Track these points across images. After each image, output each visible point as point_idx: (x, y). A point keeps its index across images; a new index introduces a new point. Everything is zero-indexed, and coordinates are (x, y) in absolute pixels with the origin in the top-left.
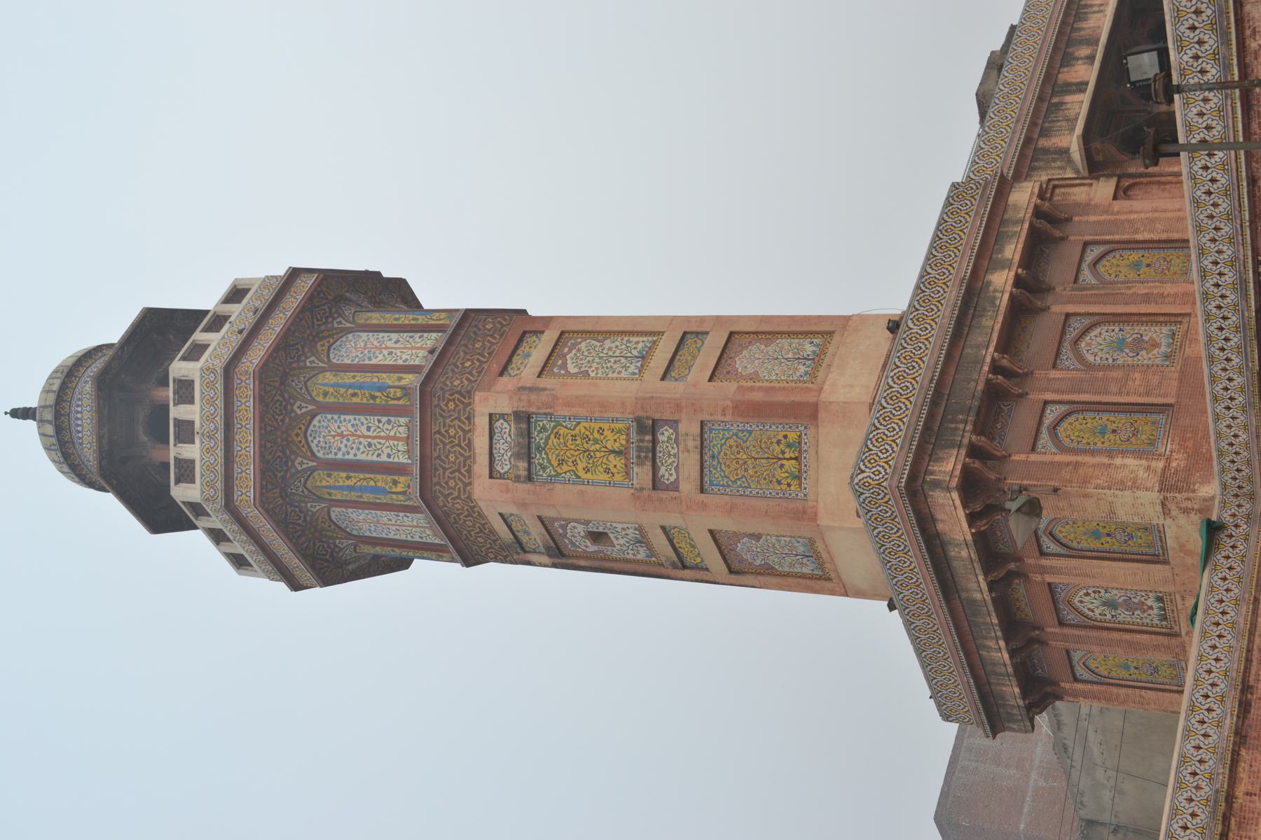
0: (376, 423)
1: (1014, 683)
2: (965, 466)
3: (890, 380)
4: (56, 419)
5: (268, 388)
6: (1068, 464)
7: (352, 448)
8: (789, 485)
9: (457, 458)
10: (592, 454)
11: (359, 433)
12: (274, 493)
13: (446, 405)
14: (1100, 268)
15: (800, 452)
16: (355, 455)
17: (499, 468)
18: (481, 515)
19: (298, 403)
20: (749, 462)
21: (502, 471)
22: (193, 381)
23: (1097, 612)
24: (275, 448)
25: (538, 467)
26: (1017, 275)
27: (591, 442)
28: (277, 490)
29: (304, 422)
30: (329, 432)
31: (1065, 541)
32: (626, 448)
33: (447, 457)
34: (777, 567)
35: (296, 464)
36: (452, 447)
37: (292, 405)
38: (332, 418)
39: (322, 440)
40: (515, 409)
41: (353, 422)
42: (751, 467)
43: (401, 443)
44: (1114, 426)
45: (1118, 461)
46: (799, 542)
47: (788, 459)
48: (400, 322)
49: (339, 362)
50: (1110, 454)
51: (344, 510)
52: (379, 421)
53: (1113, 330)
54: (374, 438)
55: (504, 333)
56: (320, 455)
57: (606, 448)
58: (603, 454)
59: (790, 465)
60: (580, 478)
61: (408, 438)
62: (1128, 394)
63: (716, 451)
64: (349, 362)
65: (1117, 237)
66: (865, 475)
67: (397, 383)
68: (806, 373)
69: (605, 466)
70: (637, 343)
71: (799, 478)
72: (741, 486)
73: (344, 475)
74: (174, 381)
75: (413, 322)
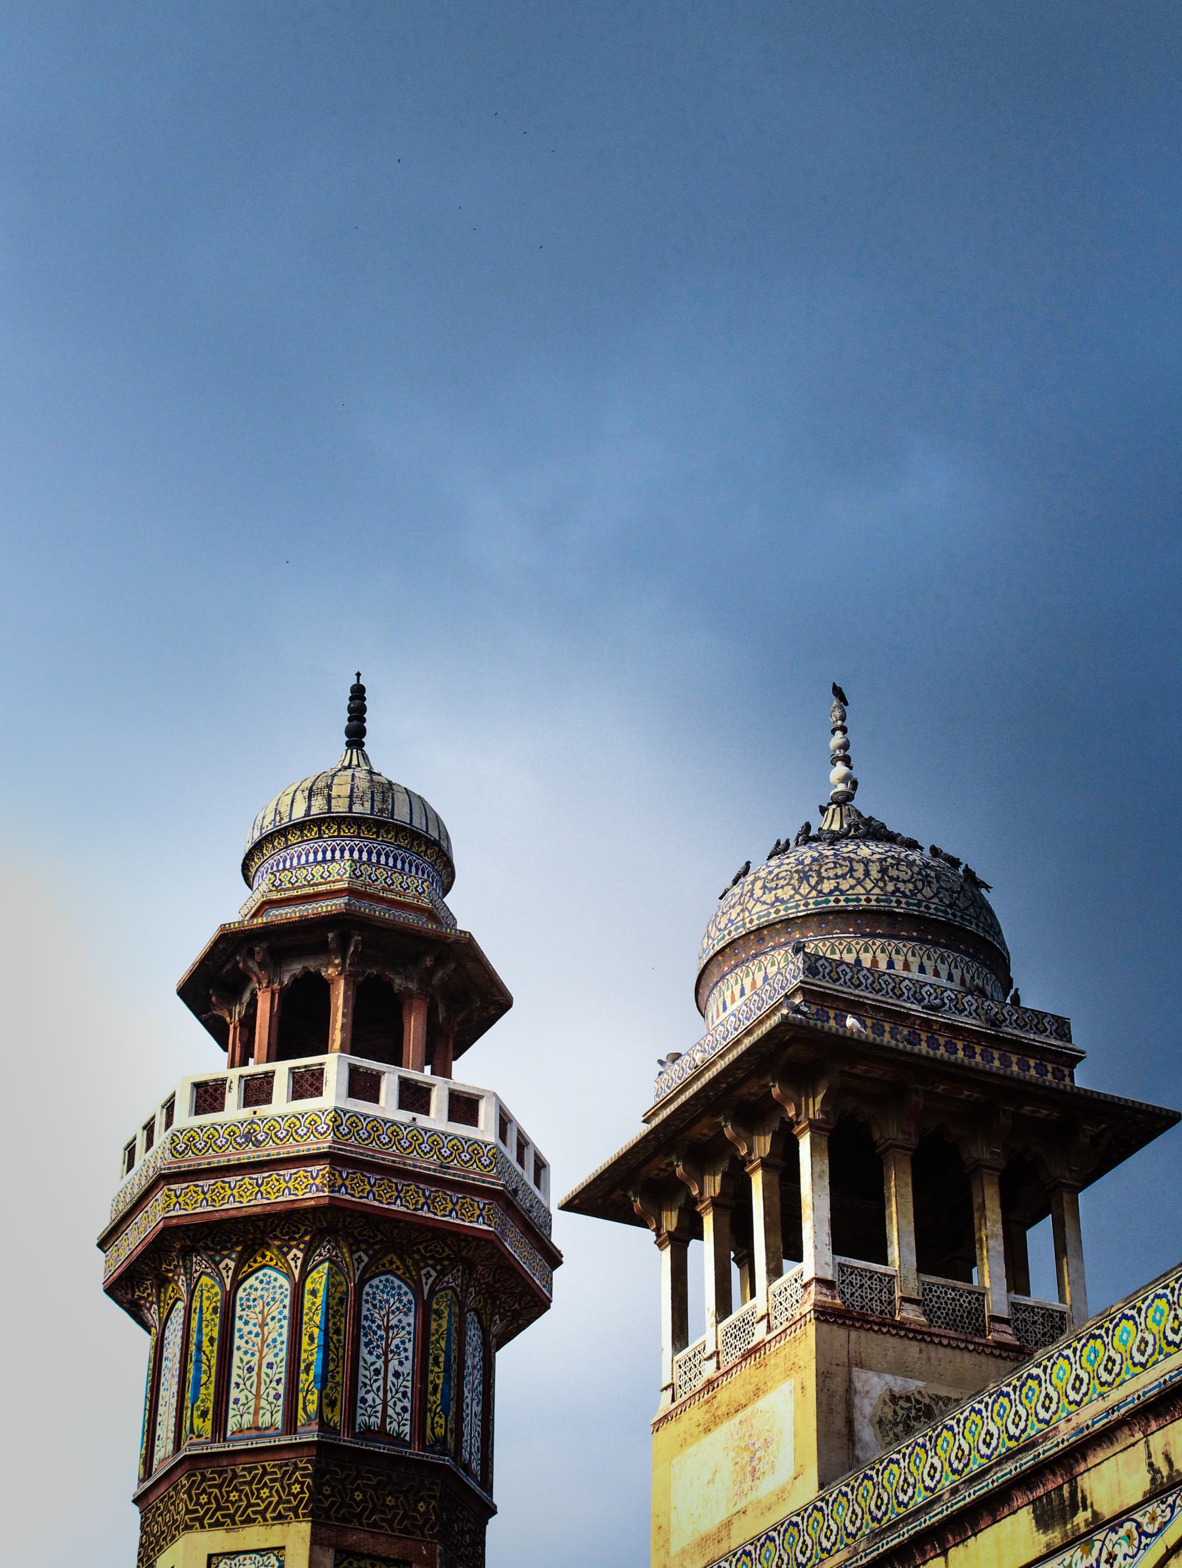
0: (277, 1377)
7: (247, 1342)
9: (233, 1503)
11: (266, 1350)
13: (297, 1481)
19: (300, 1255)
22: (321, 1094)
29: (280, 1264)
30: (268, 1304)
33: (235, 1489)
37: (297, 1247)
38: (285, 1307)
39: (259, 1293)
41: (279, 1339)
43: (251, 1417)
48: (431, 1368)
49: (364, 1297)
52: (278, 1381)
55: (409, 1533)
56: (241, 1293)
61: (258, 1428)
64: (364, 1312)
67: (325, 1401)
73: (216, 1335)
74: (321, 1064)
75: (430, 1387)
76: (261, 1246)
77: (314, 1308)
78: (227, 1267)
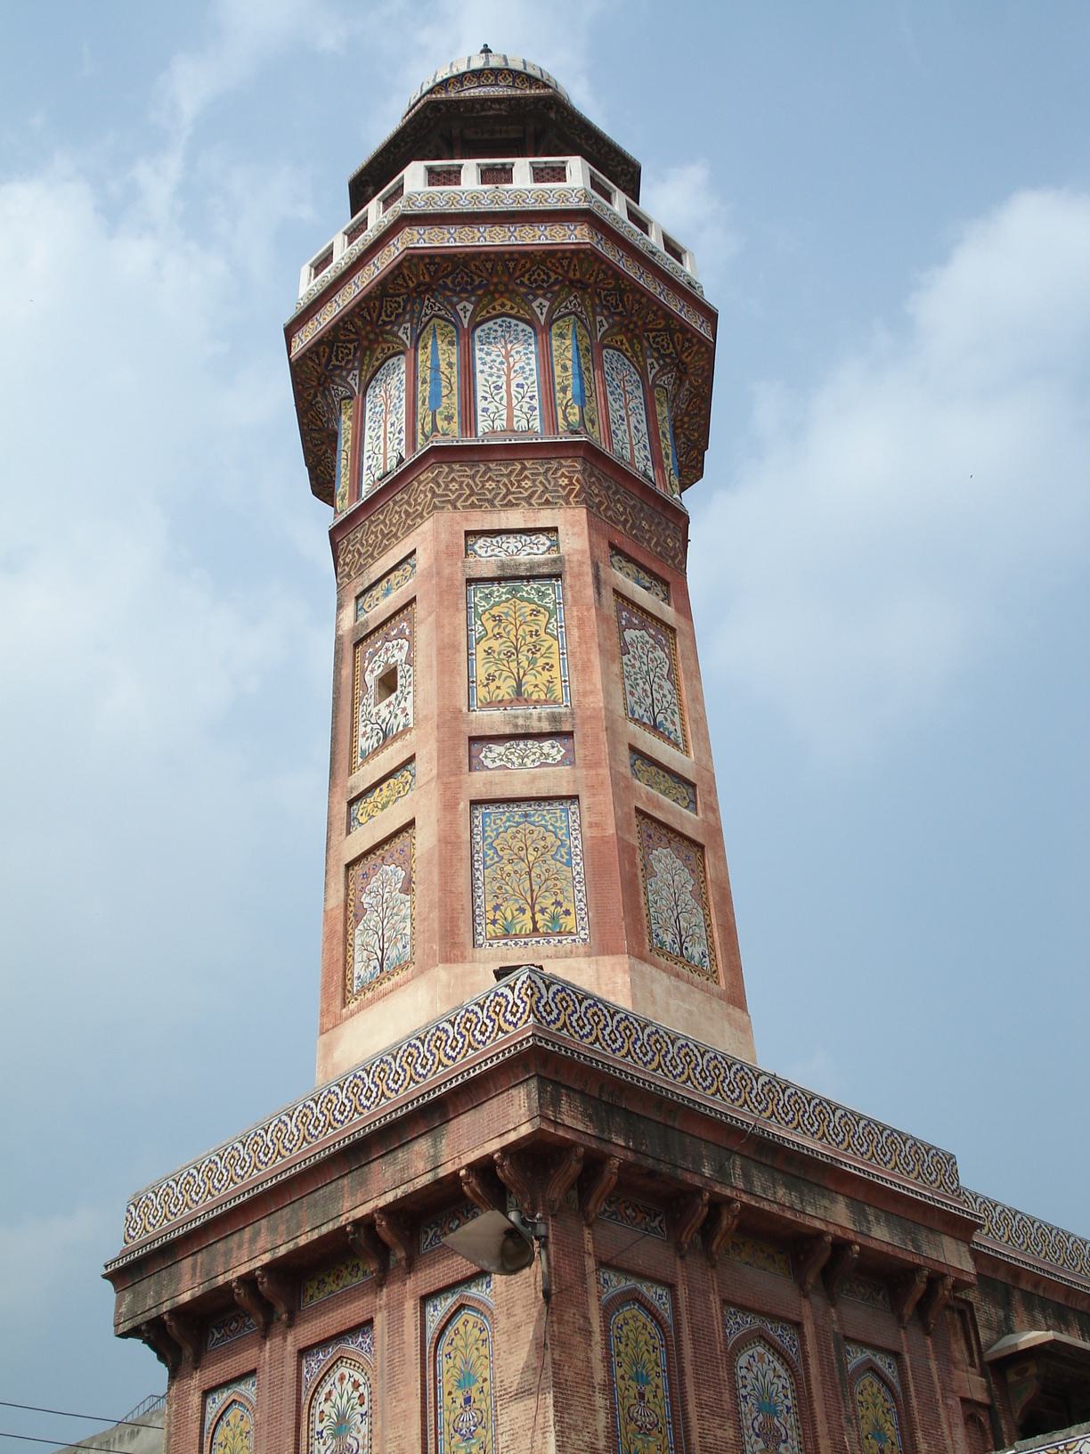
0: (531, 394)
1: (198, 1292)
2: (574, 1145)
3: (684, 1042)
4: (491, 69)
5: (565, 263)
6: (586, 1318)
8: (494, 922)
9: (490, 491)
10: (514, 657)
11: (513, 375)
12: (423, 274)
14: (868, 1379)
15: (547, 934)
16: (482, 372)
19: (547, 304)
20: (523, 865)
21: (476, 547)
23: (327, 1407)
24: (484, 275)
27: (530, 655)
28: (427, 279)
29: (522, 312)
31: (450, 1332)
32: (526, 700)
34: (360, 927)
35: (465, 303)
36: (505, 485)
37: (544, 296)
38: (530, 344)
39: (499, 334)
40: (567, 558)
41: (527, 368)
42: (516, 868)
44: (649, 1396)
45: (600, 1401)
46: (404, 947)
47: (533, 918)
50: (609, 1387)
52: (532, 398)
53: (786, 1397)
54: (508, 392)
56: (478, 332)
57: (525, 674)
58: (515, 671)
60: (477, 643)
61: (514, 431)
62: (701, 1418)
65: (914, 1402)
66: (544, 991)
68: (663, 943)
70: (673, 723)
71: (507, 934)
72: (485, 855)
73: (454, 359)
74: (563, 162)
76: (502, 294)
77: (564, 347)
78: (465, 309)
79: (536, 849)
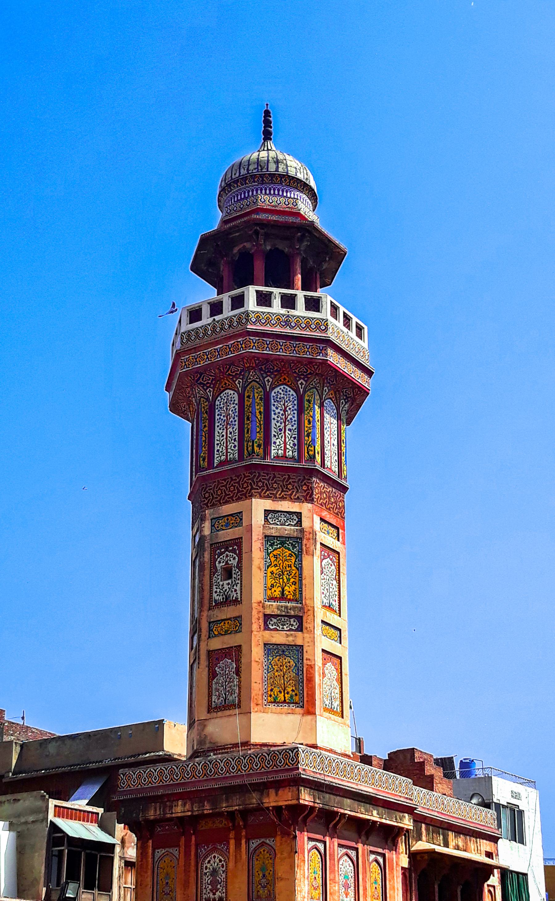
0: (294, 436)
6: (304, 857)
11: (287, 423)
17: (270, 516)
18: (239, 499)
19: (304, 383)
23: (208, 865)
25: (272, 542)
26: (377, 822)
33: (275, 482)
34: (215, 680)
39: (282, 396)
41: (294, 419)
47: (284, 696)
51: (236, 402)
58: (282, 584)
59: (281, 697)
61: (286, 457)
63: (287, 653)
67: (316, 452)
68: (326, 705)
69: (275, 584)
71: (275, 702)
79: (286, 667)
